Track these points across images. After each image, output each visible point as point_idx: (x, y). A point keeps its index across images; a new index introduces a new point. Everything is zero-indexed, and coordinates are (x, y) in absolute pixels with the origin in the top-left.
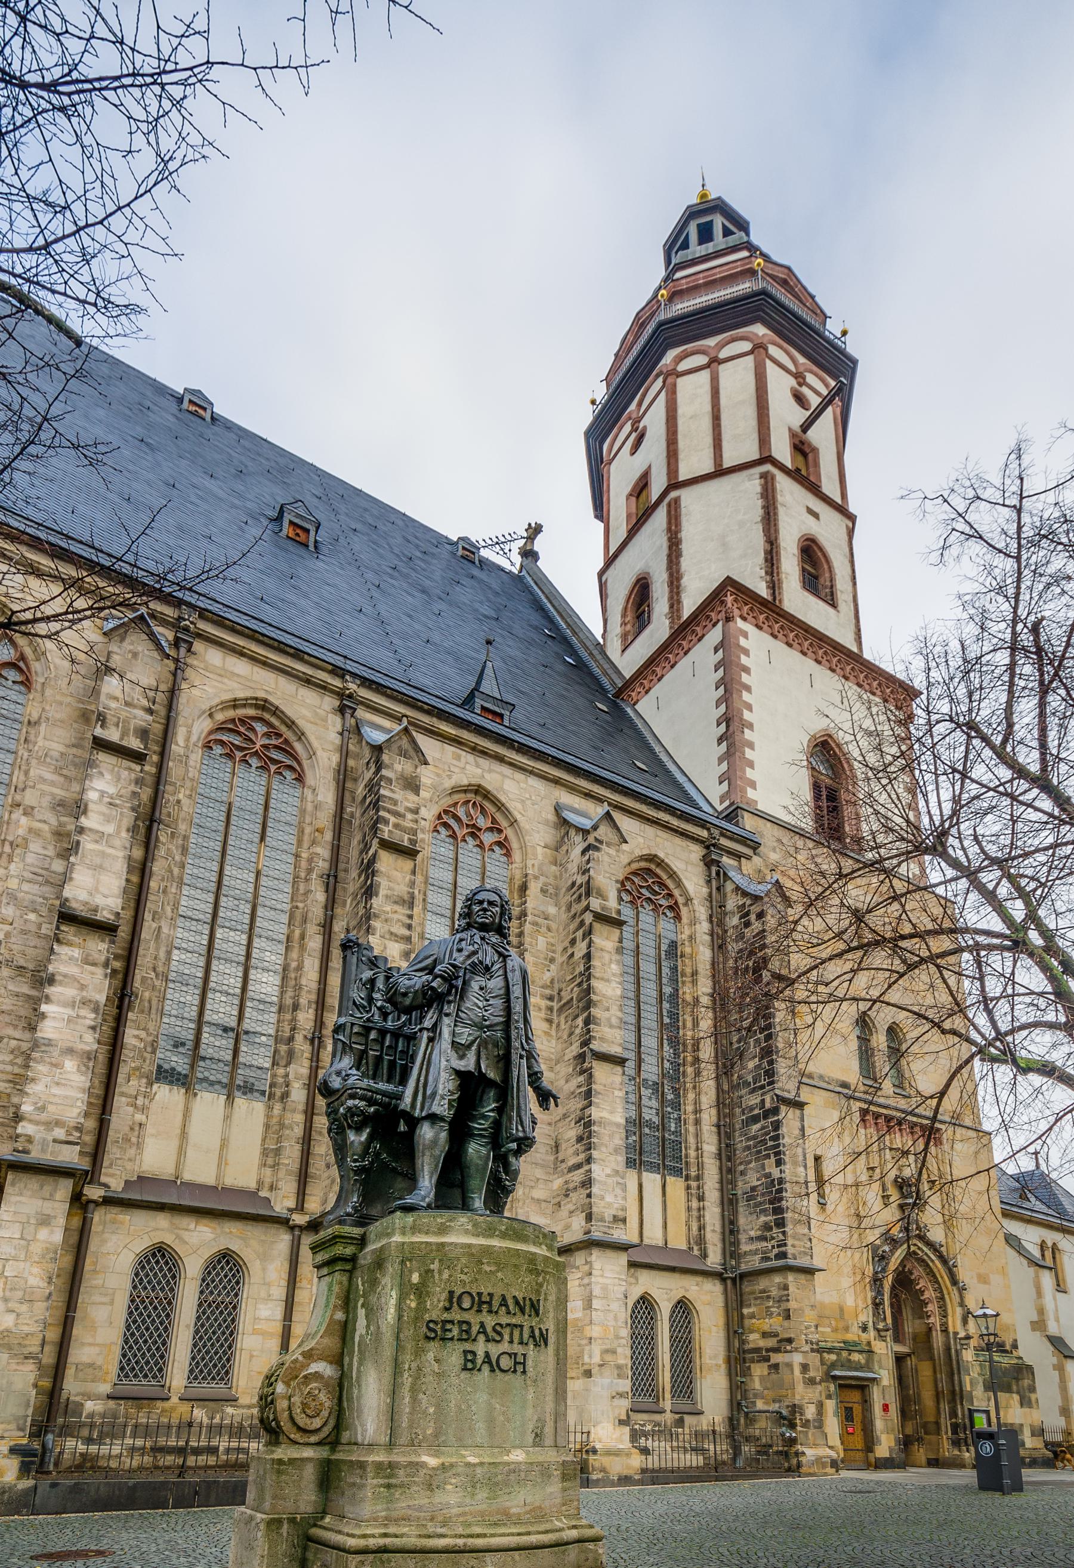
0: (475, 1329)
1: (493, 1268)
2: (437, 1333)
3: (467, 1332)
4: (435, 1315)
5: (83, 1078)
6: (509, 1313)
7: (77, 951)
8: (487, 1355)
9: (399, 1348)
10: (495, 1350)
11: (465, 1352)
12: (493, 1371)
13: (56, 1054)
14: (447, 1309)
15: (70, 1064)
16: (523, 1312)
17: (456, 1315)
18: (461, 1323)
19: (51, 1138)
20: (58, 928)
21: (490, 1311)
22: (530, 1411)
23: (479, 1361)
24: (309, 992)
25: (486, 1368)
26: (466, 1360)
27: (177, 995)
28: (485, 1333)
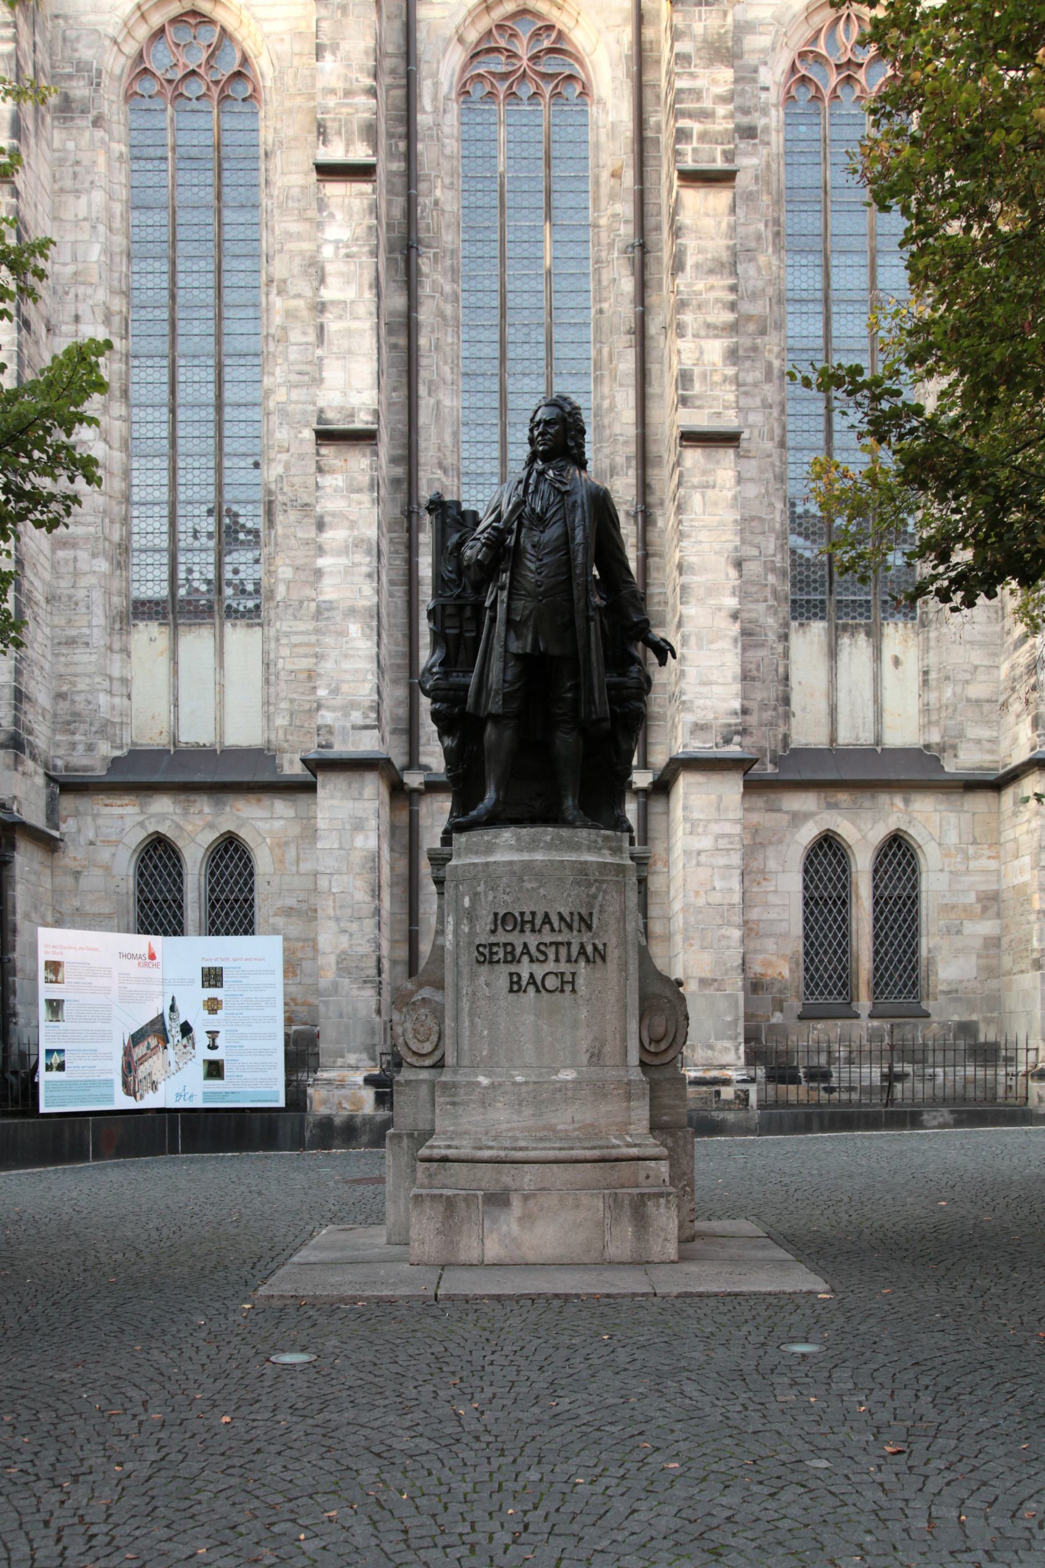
0: (519, 950)
1: (535, 885)
2: (486, 956)
3: (512, 953)
4: (484, 938)
5: (369, 644)
6: (553, 930)
7: (340, 477)
8: (532, 976)
9: (459, 974)
10: (539, 971)
11: (511, 974)
12: (538, 991)
13: (338, 619)
14: (493, 932)
15: (354, 629)
16: (570, 927)
17: (502, 937)
18: (505, 945)
19: (349, 725)
20: (318, 454)
21: (533, 930)
22: (582, 1032)
23: (524, 983)
24: (626, 443)
25: (531, 989)
26: (512, 983)
27: (473, 492)
28: (528, 953)
